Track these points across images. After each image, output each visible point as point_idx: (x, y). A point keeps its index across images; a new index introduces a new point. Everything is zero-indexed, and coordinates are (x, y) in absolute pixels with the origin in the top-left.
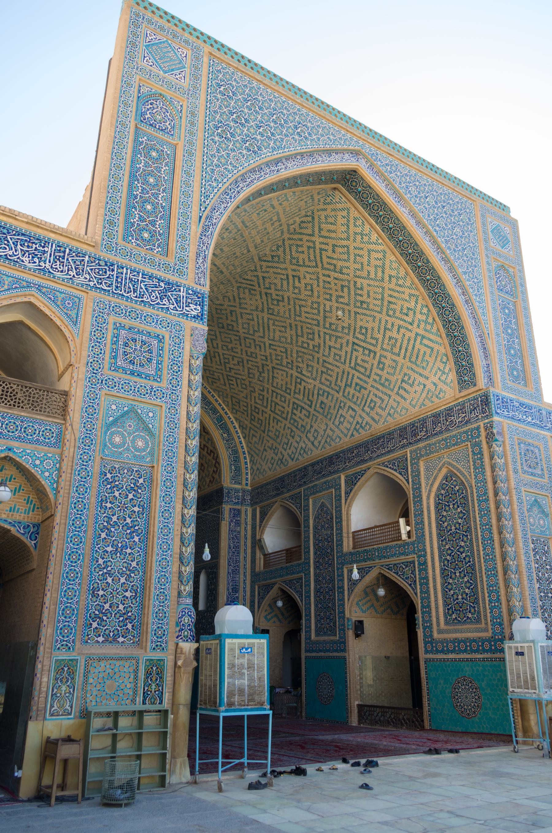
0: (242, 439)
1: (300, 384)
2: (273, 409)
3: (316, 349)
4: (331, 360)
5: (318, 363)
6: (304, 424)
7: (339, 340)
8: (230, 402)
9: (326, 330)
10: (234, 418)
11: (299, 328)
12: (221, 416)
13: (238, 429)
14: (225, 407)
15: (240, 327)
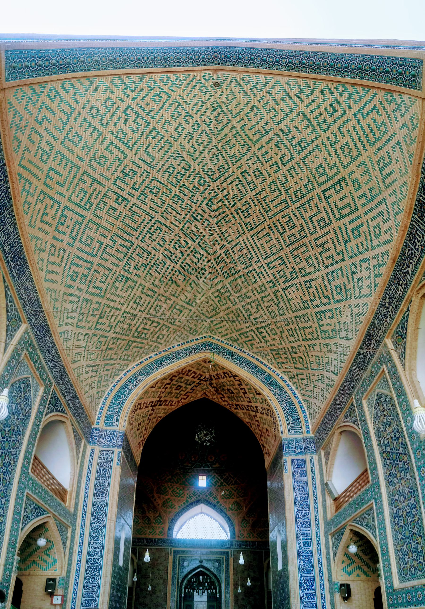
0: (296, 391)
1: (311, 287)
2: (304, 338)
3: (303, 234)
4: (320, 232)
5: (312, 248)
6: (333, 327)
7: (312, 203)
8: (273, 358)
9: (297, 205)
10: (283, 372)
11: (278, 224)
12: (269, 375)
13: (289, 382)
14: (271, 366)
15: (239, 264)
